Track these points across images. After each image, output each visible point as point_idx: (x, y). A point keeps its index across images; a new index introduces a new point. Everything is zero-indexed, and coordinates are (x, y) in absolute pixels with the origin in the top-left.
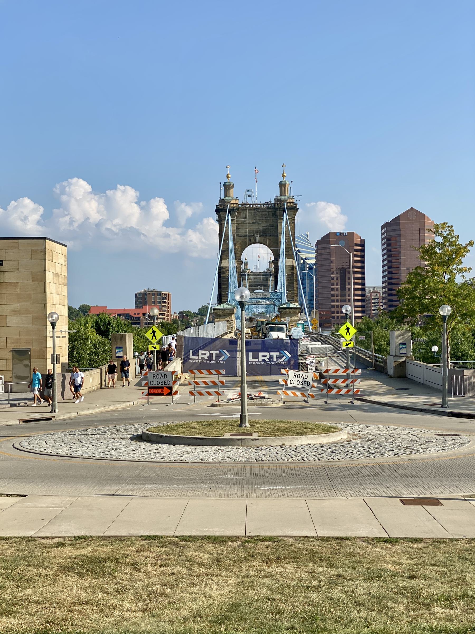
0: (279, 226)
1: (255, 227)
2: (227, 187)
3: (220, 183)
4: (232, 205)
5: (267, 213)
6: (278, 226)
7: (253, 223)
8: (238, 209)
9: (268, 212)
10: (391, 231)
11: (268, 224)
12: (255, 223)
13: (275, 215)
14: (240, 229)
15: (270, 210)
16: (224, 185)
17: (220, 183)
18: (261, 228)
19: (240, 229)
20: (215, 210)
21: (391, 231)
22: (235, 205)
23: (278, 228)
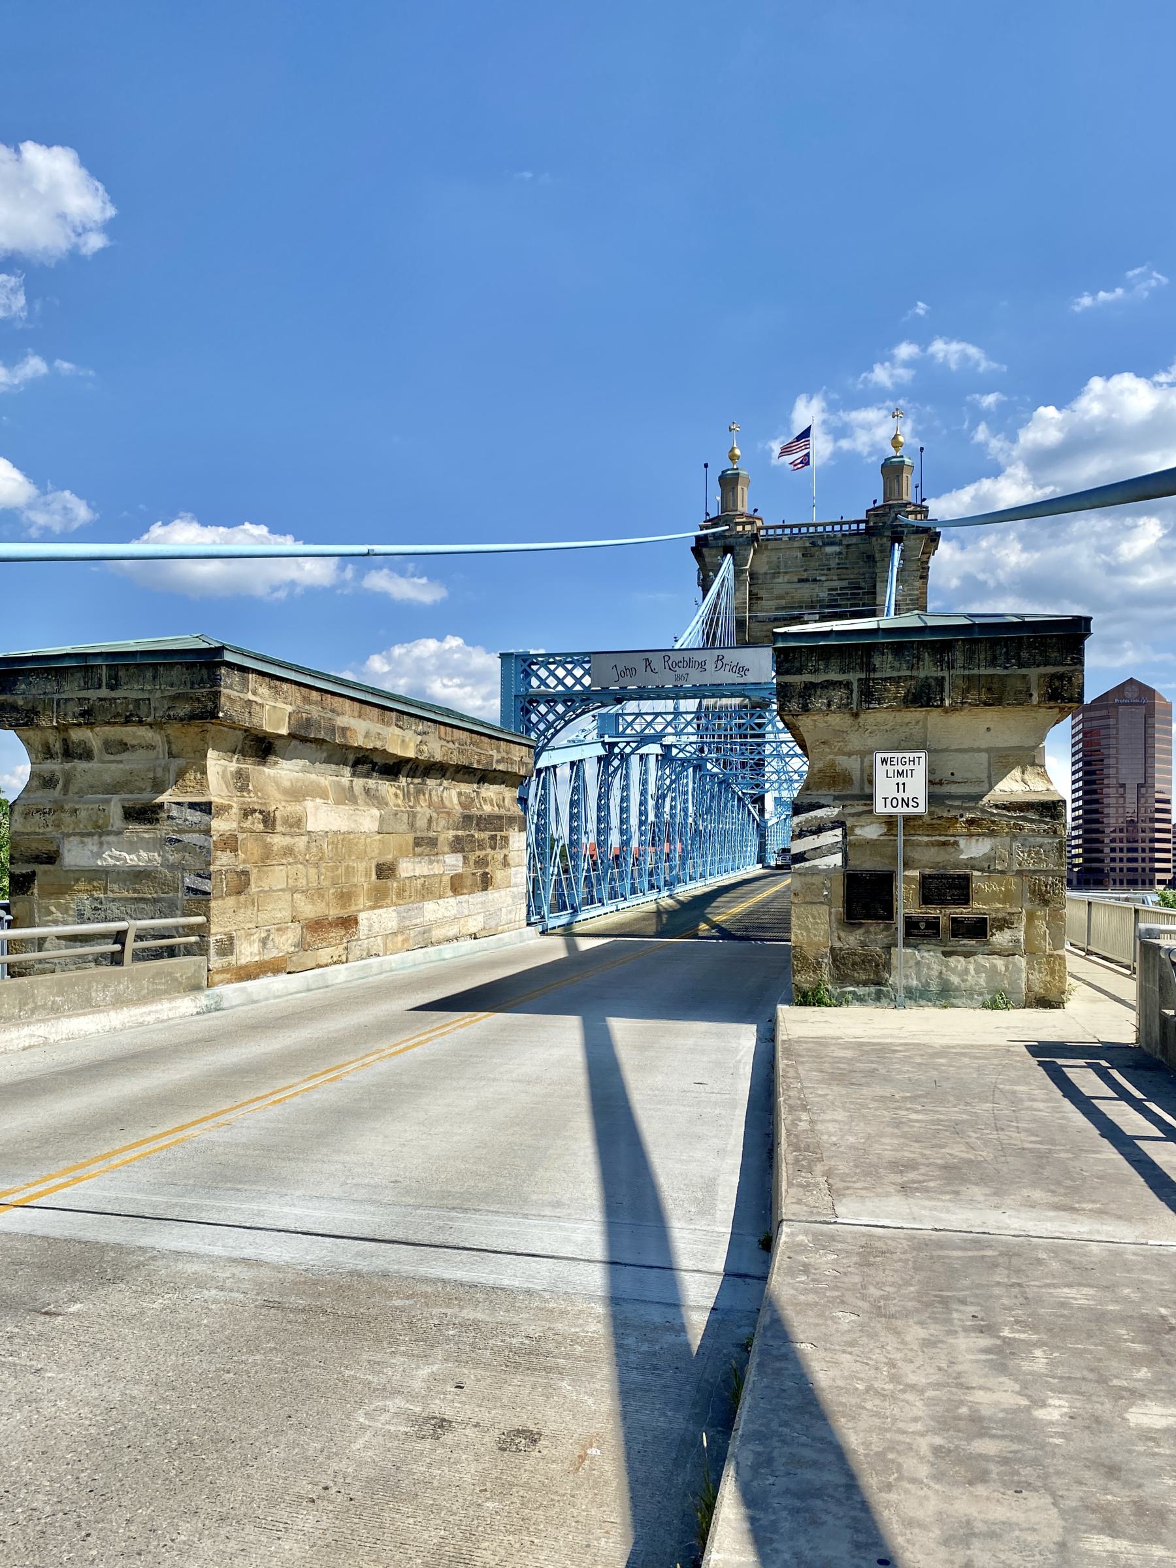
0: (878, 585)
1: (805, 592)
2: (728, 482)
3: (706, 466)
4: (740, 528)
5: (844, 551)
6: (875, 586)
7: (801, 581)
8: (755, 537)
9: (848, 546)
10: (1092, 719)
11: (845, 584)
12: (807, 580)
13: (870, 559)
14: (761, 598)
15: (854, 540)
16: (720, 478)
17: (706, 466)
18: (824, 595)
19: (761, 598)
20: (692, 549)
21: (1092, 719)
22: (748, 528)
23: (874, 593)
